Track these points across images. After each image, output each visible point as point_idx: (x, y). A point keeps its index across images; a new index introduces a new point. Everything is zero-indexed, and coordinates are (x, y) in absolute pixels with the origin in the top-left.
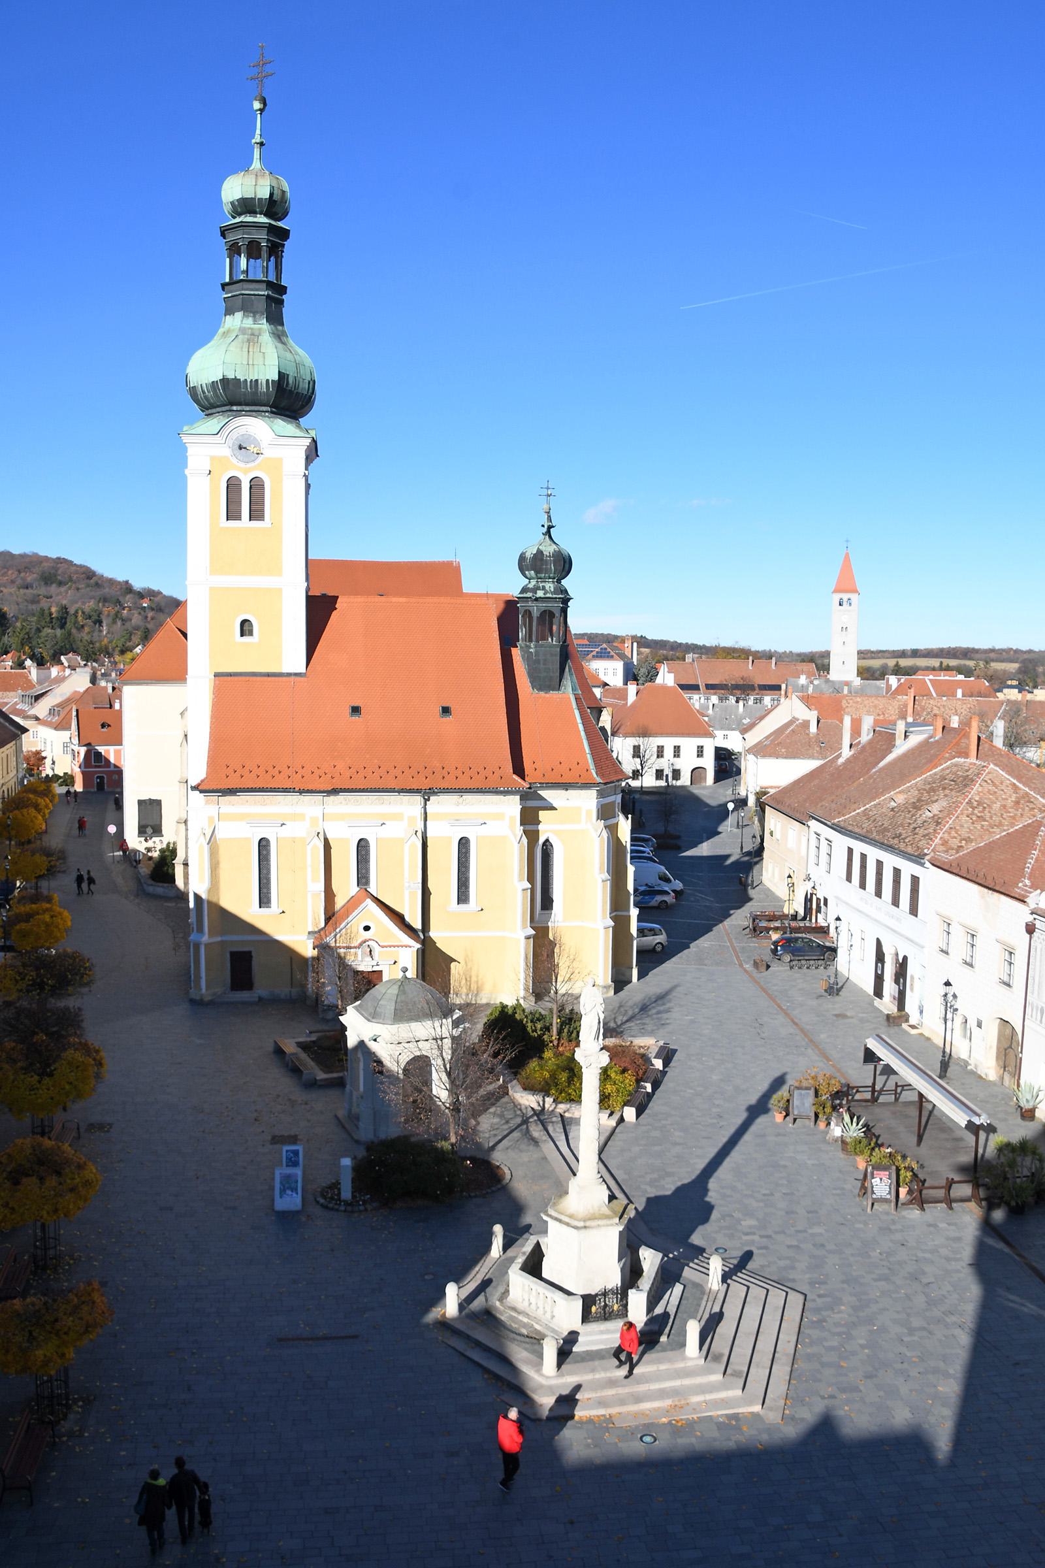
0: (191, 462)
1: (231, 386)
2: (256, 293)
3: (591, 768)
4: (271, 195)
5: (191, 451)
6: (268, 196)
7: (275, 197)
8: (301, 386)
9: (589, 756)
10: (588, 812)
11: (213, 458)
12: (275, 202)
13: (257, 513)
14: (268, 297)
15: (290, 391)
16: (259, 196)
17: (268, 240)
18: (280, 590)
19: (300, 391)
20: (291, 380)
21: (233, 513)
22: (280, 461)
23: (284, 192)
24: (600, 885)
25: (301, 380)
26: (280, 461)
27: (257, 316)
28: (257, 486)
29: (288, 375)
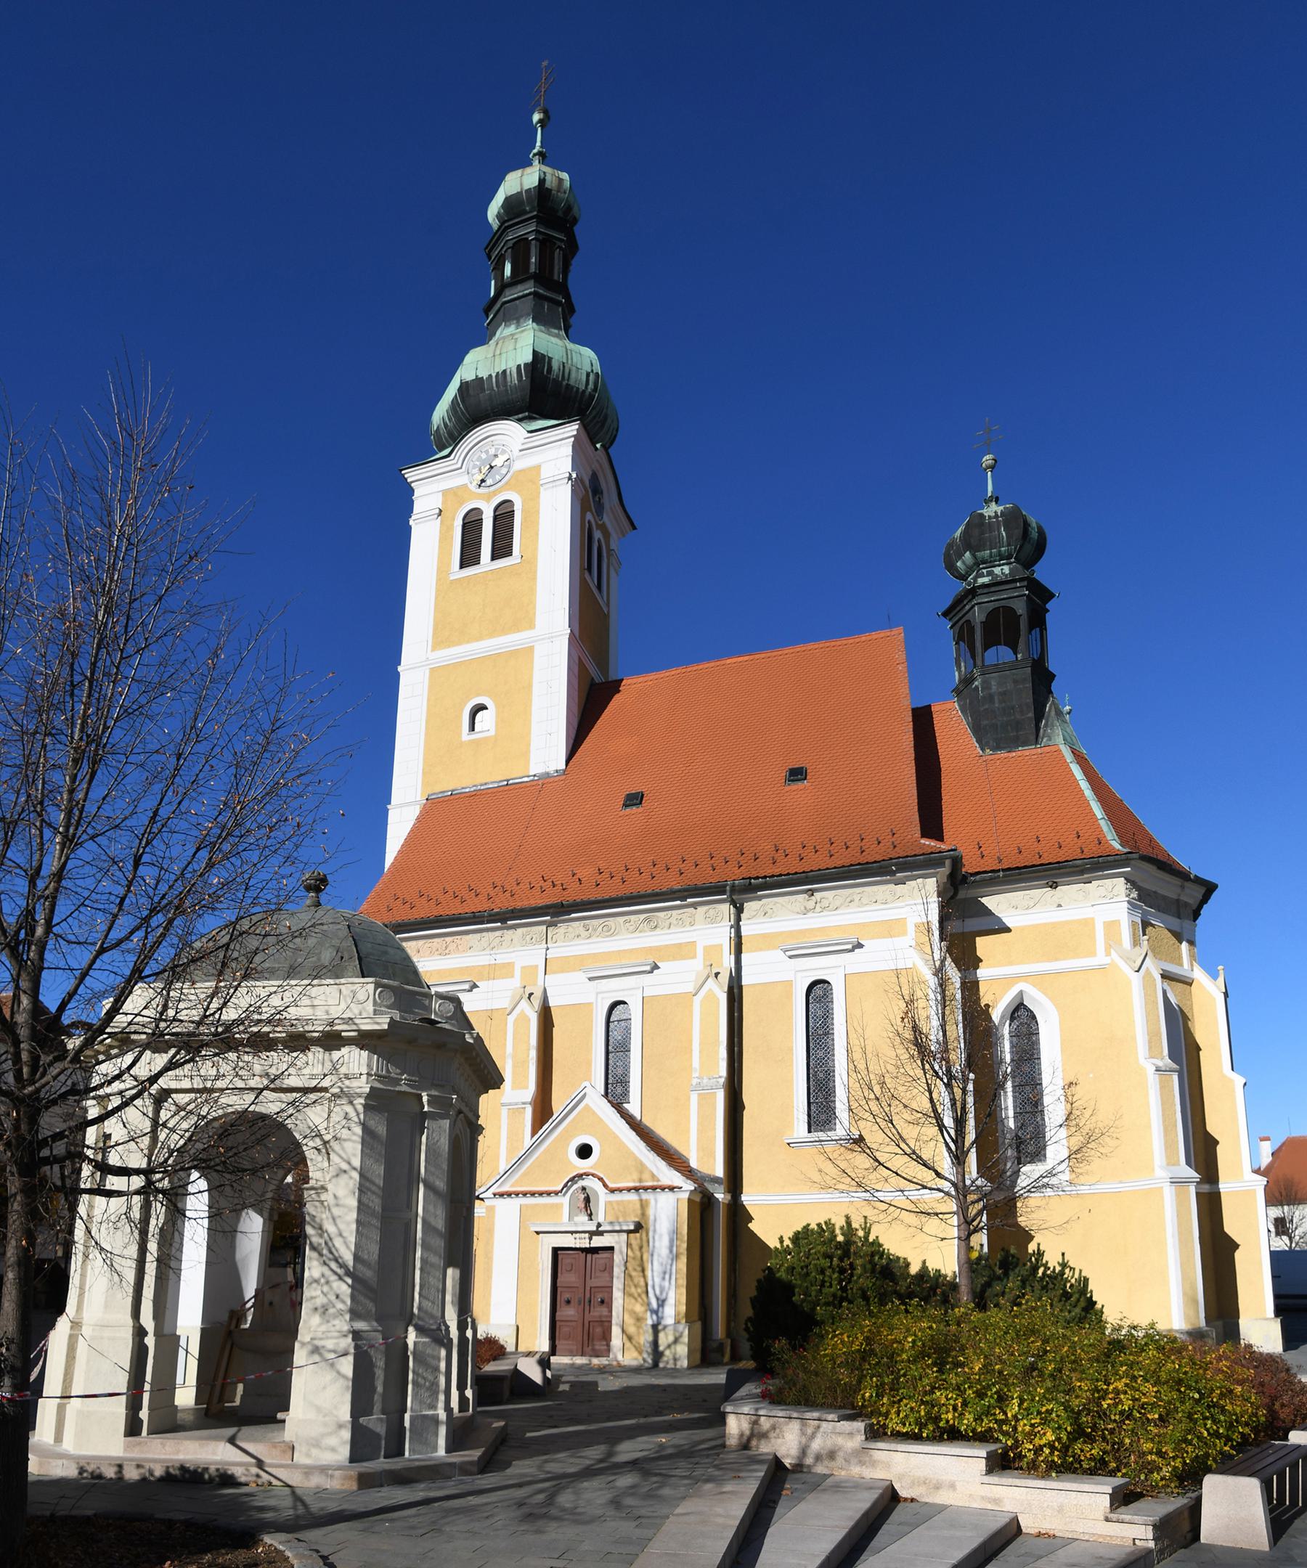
0: (418, 507)
1: (471, 392)
2: (521, 294)
3: (1109, 837)
4: (542, 181)
5: (420, 489)
6: (536, 183)
7: (548, 185)
8: (573, 375)
9: (1105, 825)
10: (1111, 926)
11: (445, 493)
12: (549, 191)
13: (502, 548)
14: (535, 294)
15: (557, 382)
16: (526, 187)
17: (537, 231)
18: (531, 650)
19: (572, 382)
20: (555, 365)
21: (469, 556)
22: (537, 468)
23: (561, 181)
24: (1152, 1079)
25: (574, 369)
26: (537, 468)
27: (522, 320)
28: (504, 516)
29: (550, 359)
